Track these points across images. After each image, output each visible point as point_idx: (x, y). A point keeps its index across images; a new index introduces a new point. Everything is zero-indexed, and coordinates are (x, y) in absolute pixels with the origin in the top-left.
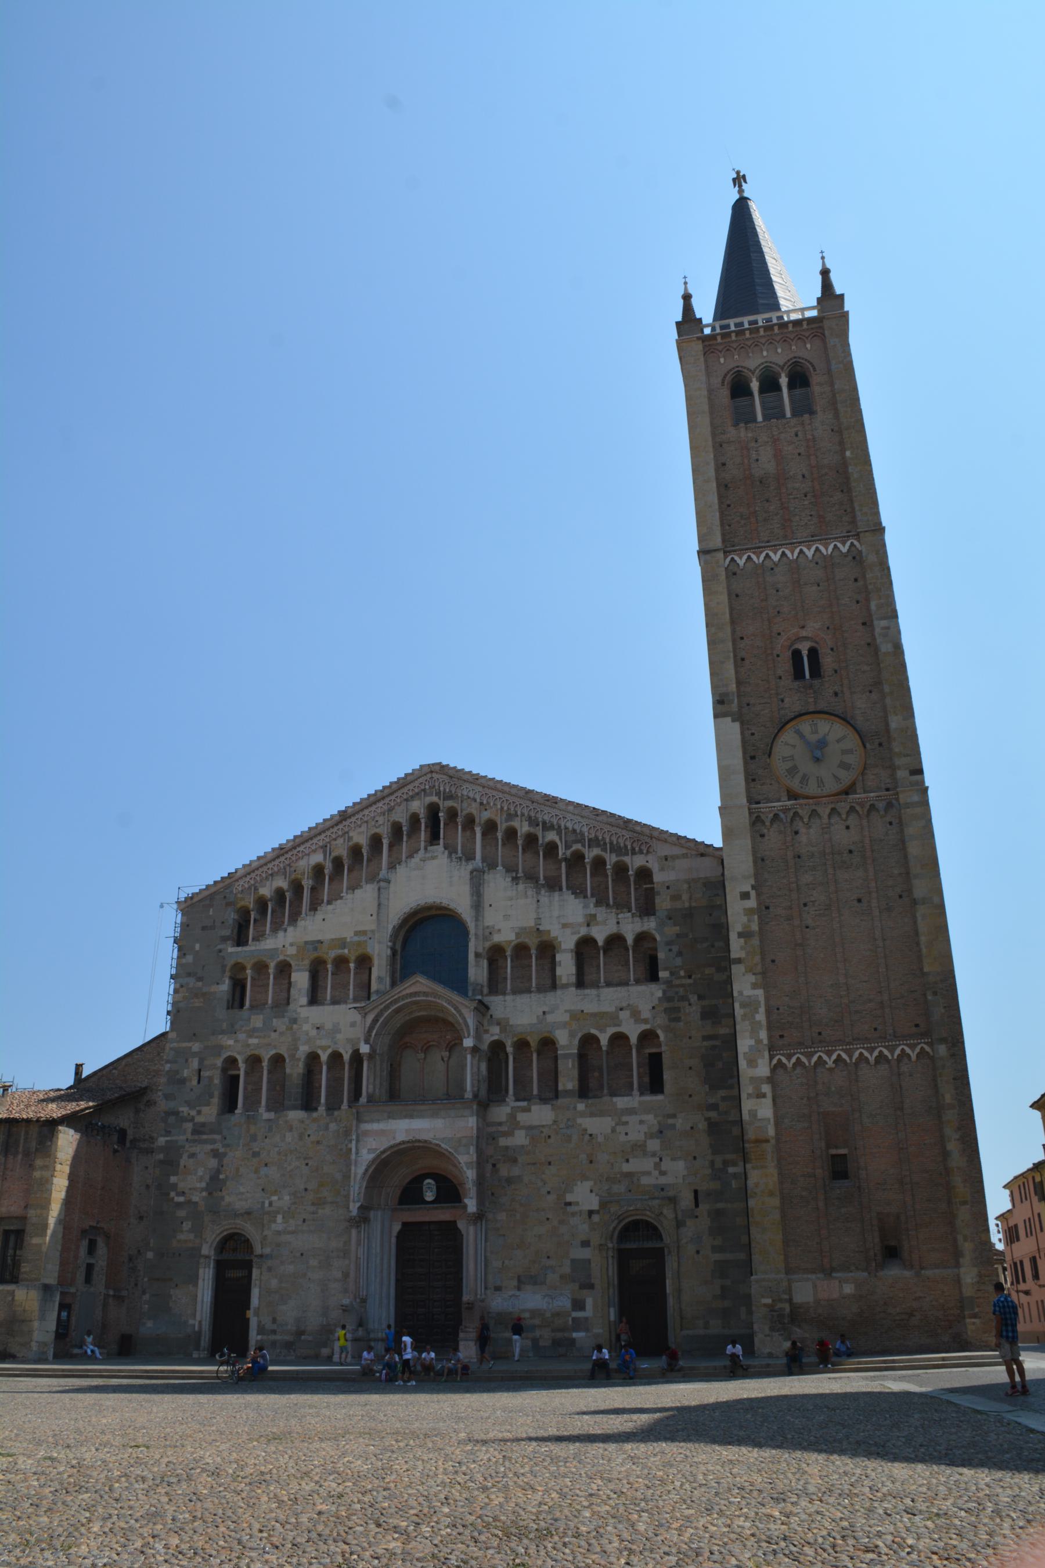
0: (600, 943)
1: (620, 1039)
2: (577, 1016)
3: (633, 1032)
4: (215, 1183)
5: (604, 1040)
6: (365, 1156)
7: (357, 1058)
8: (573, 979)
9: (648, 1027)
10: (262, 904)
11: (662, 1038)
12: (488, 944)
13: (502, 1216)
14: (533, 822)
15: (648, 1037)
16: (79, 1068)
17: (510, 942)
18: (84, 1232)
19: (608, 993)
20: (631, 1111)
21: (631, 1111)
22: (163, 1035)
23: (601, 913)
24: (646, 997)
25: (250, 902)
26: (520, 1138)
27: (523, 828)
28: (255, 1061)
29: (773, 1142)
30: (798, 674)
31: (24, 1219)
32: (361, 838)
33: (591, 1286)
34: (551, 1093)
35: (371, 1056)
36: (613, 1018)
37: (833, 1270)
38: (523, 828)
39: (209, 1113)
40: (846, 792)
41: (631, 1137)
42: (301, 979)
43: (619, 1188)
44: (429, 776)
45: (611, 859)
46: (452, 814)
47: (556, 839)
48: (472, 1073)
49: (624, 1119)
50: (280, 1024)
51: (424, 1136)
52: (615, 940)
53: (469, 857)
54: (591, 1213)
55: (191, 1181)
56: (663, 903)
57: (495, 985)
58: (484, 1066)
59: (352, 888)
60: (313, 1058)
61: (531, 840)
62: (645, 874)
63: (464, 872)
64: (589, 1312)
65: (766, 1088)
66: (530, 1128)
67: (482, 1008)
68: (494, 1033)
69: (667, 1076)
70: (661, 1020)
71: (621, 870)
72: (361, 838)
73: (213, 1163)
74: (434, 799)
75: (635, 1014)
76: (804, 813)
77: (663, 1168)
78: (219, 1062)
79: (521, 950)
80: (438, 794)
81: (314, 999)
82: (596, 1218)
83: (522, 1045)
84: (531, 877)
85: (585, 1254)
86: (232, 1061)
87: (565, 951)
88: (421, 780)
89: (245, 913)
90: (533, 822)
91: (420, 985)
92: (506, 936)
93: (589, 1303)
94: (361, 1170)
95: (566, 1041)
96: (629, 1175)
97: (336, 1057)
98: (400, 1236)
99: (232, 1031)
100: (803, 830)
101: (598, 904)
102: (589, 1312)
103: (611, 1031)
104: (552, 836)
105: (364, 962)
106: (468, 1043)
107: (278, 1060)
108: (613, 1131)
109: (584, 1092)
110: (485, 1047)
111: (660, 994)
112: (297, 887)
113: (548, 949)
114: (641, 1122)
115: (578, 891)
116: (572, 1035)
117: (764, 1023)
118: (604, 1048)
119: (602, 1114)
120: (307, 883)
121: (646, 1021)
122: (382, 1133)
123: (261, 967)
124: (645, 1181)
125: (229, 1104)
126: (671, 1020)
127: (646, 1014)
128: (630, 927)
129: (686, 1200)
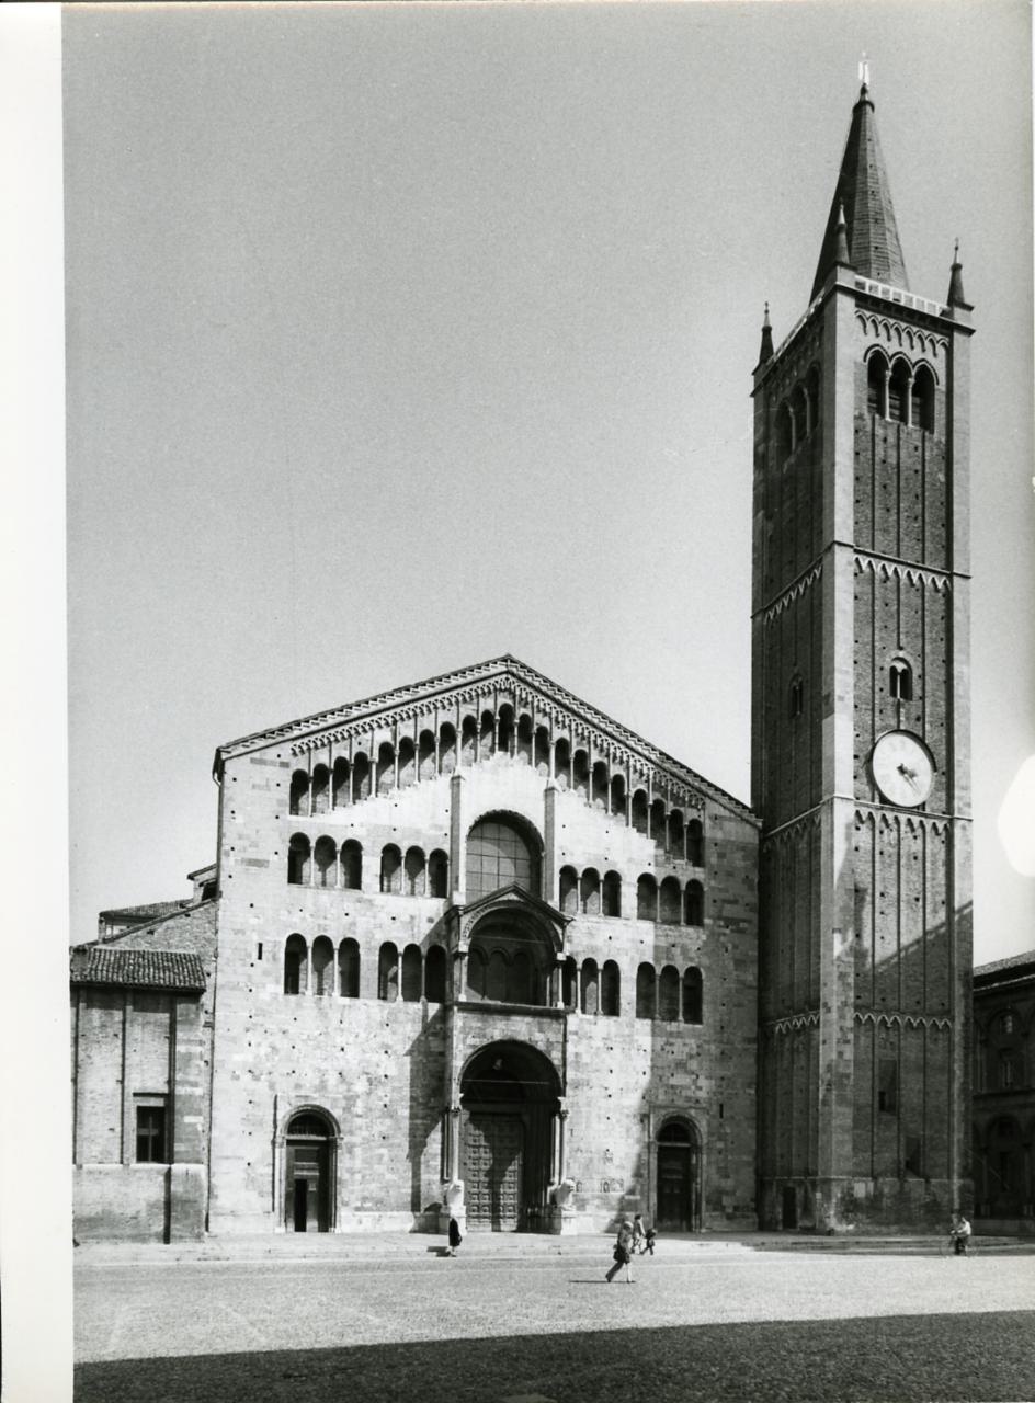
0: (659, 883)
3: (682, 967)
9: (693, 965)
11: (704, 976)
15: (693, 972)
17: (581, 866)
20: (679, 1035)
21: (679, 1035)
24: (692, 938)
29: (852, 1077)
30: (894, 694)
34: (612, 1008)
37: (880, 1174)
40: (917, 807)
41: (678, 1056)
44: (504, 676)
45: (670, 807)
46: (526, 720)
47: (624, 774)
49: (672, 1040)
52: (671, 882)
56: (711, 857)
61: (601, 768)
62: (696, 825)
65: (851, 1036)
70: (705, 961)
71: (677, 816)
74: (510, 702)
75: (685, 950)
76: (890, 816)
77: (699, 1084)
79: (591, 873)
80: (512, 694)
87: (629, 884)
88: (495, 679)
96: (672, 1087)
100: (886, 831)
103: (664, 963)
107: (350, 946)
108: (663, 1049)
111: (704, 937)
113: (613, 879)
114: (685, 1045)
115: (641, 830)
117: (852, 985)
118: (658, 978)
121: (691, 959)
123: (326, 843)
128: (685, 872)
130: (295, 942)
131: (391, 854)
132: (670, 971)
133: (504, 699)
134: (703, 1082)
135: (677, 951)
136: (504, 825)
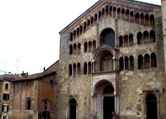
1: (147, 55)
2: (137, 50)
4: (69, 90)
5: (143, 56)
6: (94, 83)
7: (93, 63)
8: (137, 42)
10: (75, 31)
12: (119, 36)
13: (123, 95)
14: (128, 7)
15: (153, 55)
16: (44, 68)
18: (43, 101)
19: (143, 45)
22: (58, 61)
23: (142, 27)
25: (72, 31)
26: (126, 78)
27: (126, 9)
28: (75, 65)
31: (30, 98)
32: (93, 15)
33: (140, 110)
34: (132, 69)
35: (95, 62)
36: (146, 51)
38: (126, 9)
39: (67, 76)
42: (82, 47)
43: (147, 89)
45: (145, 14)
46: (111, 7)
48: (115, 66)
50: (79, 56)
51: (106, 79)
52: (146, 32)
53: (115, 17)
54: (141, 94)
55: (65, 89)
57: (121, 45)
58: (118, 63)
59: (92, 27)
60: (85, 63)
61: (128, 11)
62: (152, 16)
63: (113, 21)
64: (140, 116)
66: (128, 76)
67: (117, 51)
68: (120, 56)
69: (157, 64)
70: (156, 50)
71: (147, 15)
72: (93, 15)
73: (68, 86)
78: (68, 65)
79: (126, 36)
81: (85, 50)
82: (142, 95)
83: (126, 58)
84: (127, 20)
85: (140, 103)
86: (70, 65)
89: (72, 34)
90: (128, 7)
91: (104, 46)
92: (122, 34)
93: (140, 114)
94: (94, 86)
95: (135, 57)
97: (90, 63)
98: (104, 100)
99: (70, 59)
101: (142, 24)
102: (140, 116)
103: (145, 53)
104: (132, 10)
105: (94, 42)
106: (114, 58)
107: (79, 64)
109: (140, 67)
110: (118, 59)
112: (81, 27)
113: (131, 36)
115: (137, 22)
116: (137, 55)
119: (143, 72)
120: (83, 25)
122: (96, 79)
123: (75, 45)
124: (152, 87)
125: (70, 74)
126: (158, 50)
127: (153, 49)
128: (149, 30)
129: (161, 91)
130: (70, 66)
131: (86, 44)
132: (147, 55)
133: (106, 5)
134: (157, 83)
135: (148, 50)
136: (107, 32)
